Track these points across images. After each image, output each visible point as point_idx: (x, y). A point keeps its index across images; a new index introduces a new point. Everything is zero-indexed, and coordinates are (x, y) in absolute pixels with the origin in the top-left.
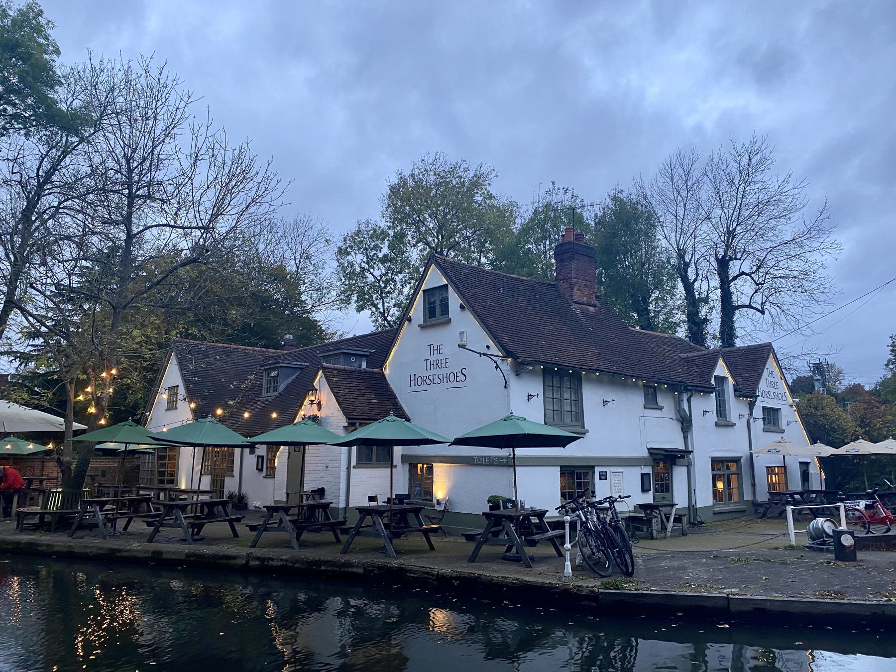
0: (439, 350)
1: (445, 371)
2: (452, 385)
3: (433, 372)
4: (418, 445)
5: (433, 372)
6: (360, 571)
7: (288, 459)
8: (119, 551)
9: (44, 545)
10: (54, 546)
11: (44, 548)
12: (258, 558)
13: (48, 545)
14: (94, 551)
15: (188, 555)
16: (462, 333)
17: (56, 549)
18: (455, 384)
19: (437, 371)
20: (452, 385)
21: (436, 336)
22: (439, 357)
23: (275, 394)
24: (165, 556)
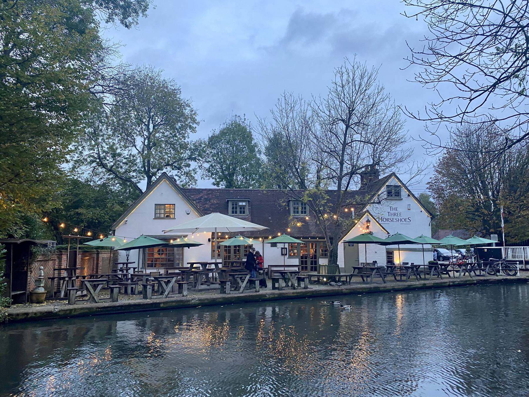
0: (396, 209)
1: (399, 218)
2: (403, 223)
3: (392, 217)
4: (405, 244)
5: (394, 217)
6: (476, 282)
7: (344, 249)
8: (412, 285)
9: (383, 287)
10: (386, 287)
11: (383, 288)
12: (452, 282)
13: (384, 287)
14: (403, 287)
15: (434, 284)
16: (409, 205)
17: (387, 288)
18: (405, 222)
19: (395, 217)
20: (403, 223)
21: (394, 204)
22: (396, 212)
23: (244, 215)
24: (427, 285)
